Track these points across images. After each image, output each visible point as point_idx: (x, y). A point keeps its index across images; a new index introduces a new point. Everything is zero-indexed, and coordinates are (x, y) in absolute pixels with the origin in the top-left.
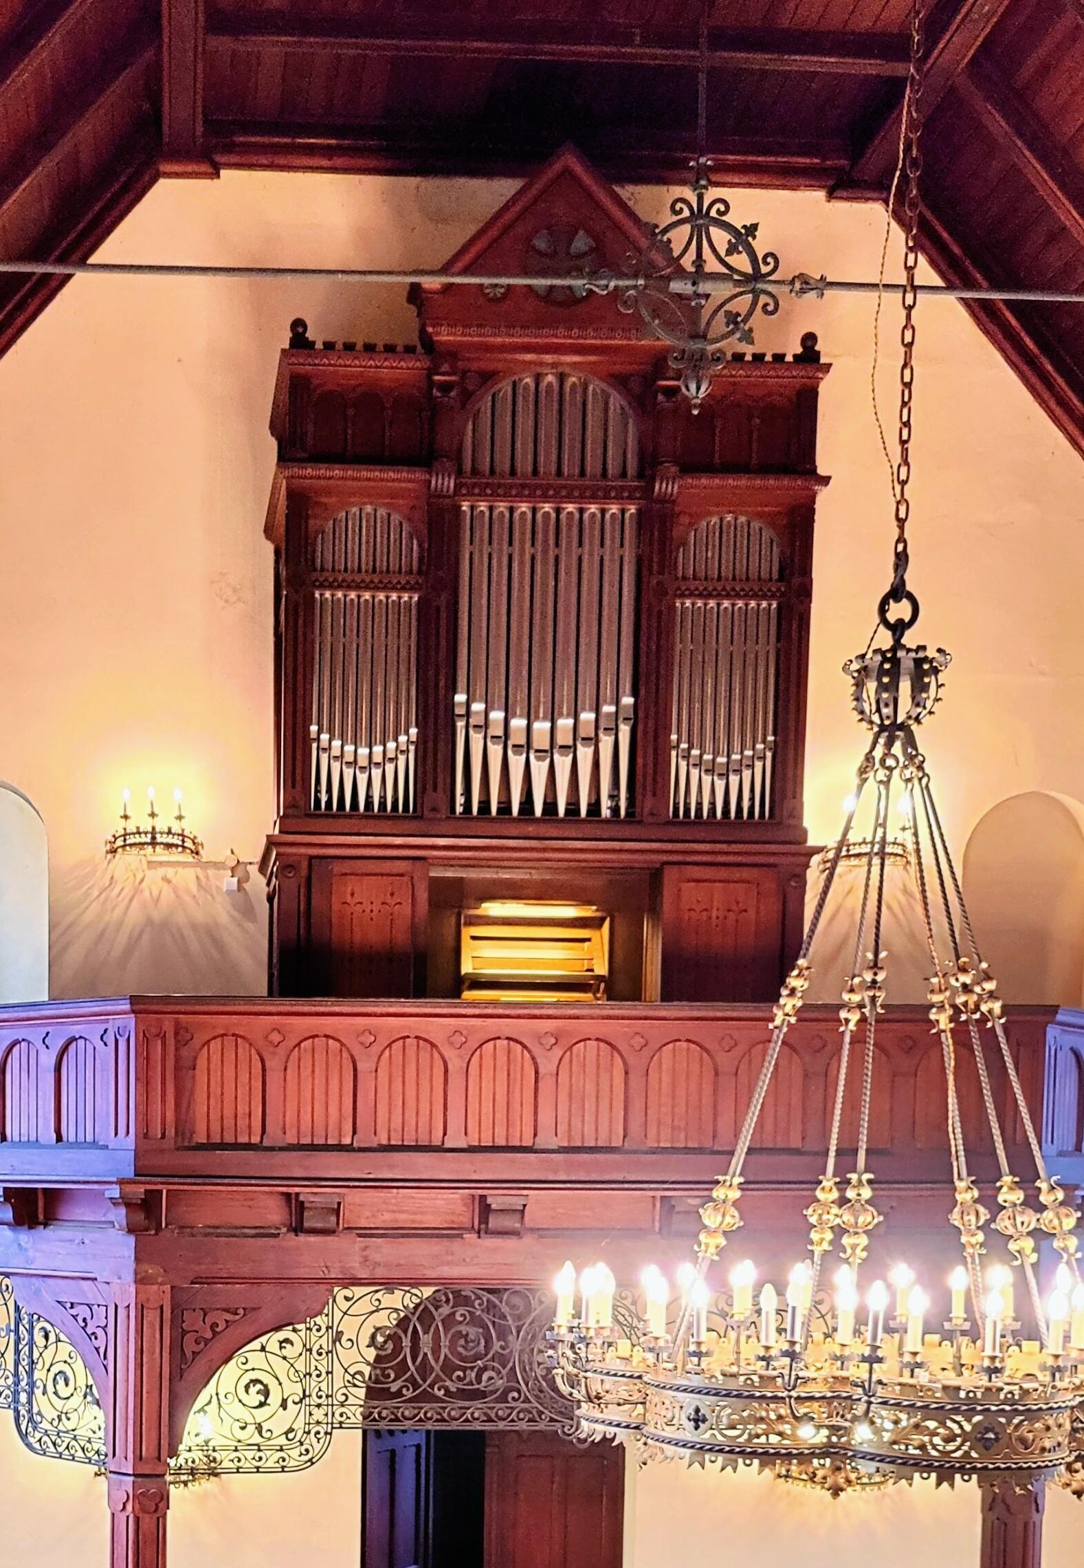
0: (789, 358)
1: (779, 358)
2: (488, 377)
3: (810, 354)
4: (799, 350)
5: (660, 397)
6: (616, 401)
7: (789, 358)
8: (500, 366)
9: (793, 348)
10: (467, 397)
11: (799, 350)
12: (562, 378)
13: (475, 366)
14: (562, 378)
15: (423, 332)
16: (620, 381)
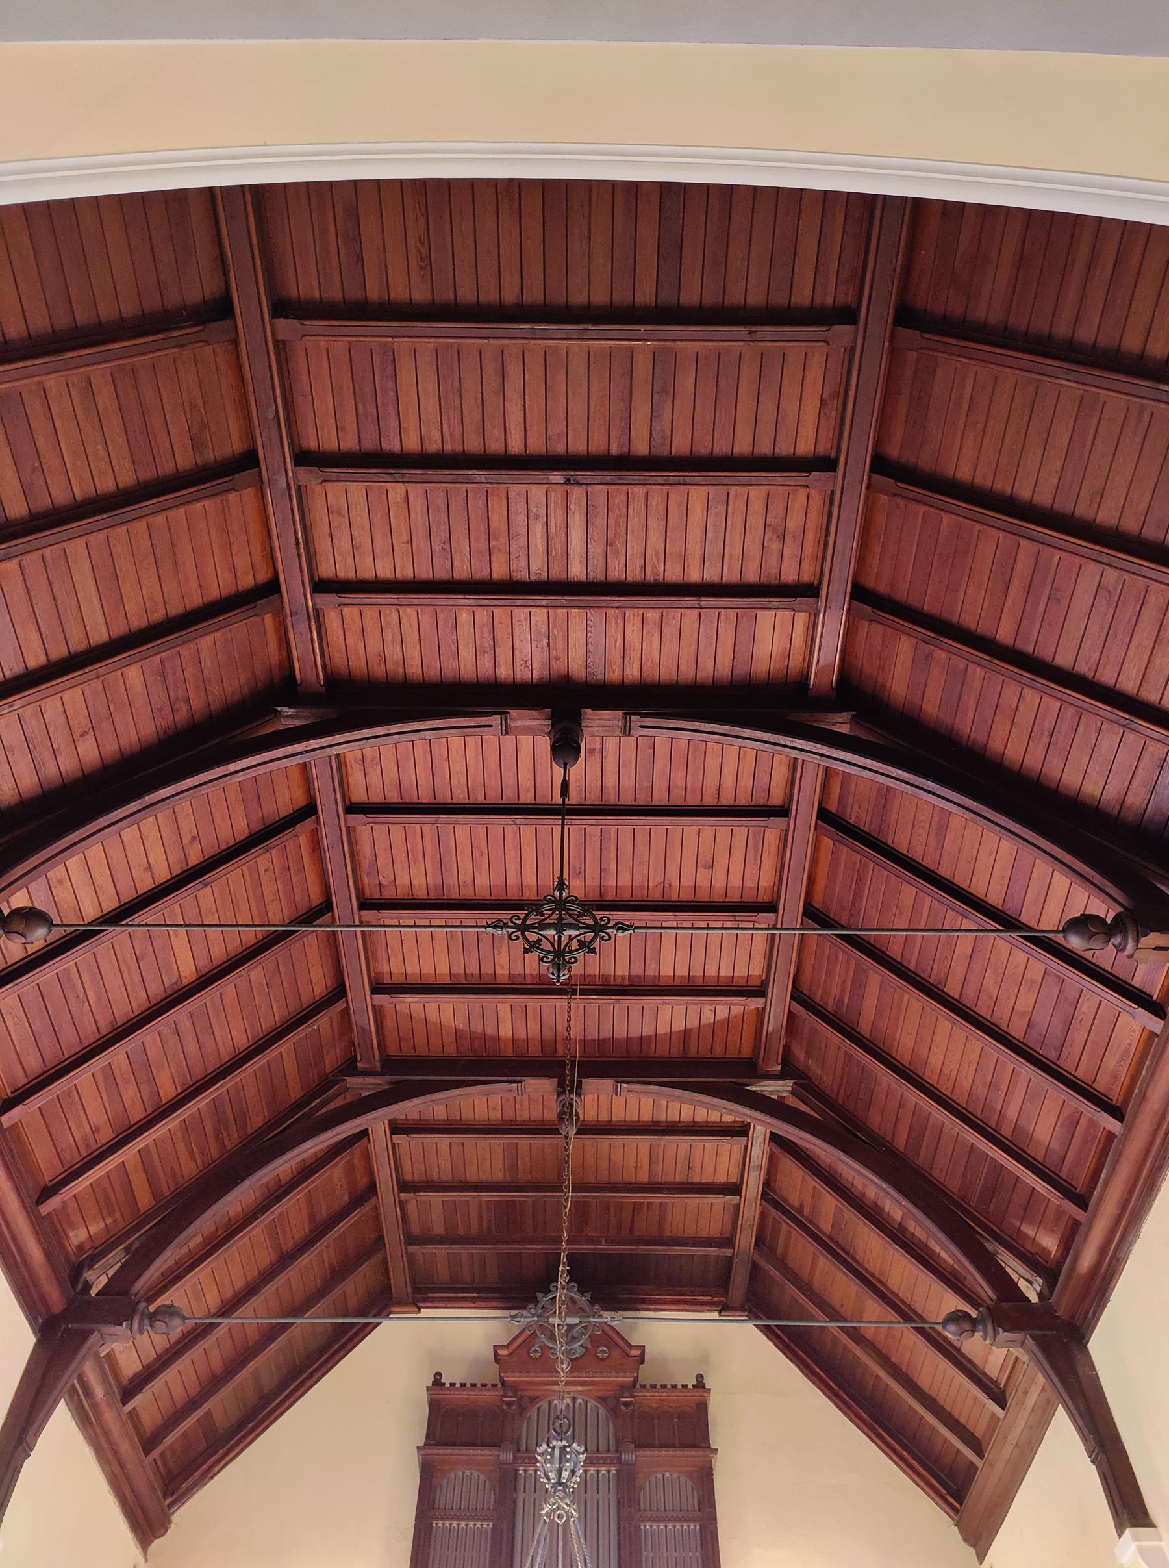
0: (690, 1387)
1: (685, 1386)
2: (533, 1400)
3: (700, 1384)
4: (695, 1382)
5: (623, 1407)
6: (602, 1411)
7: (690, 1387)
8: (536, 1394)
9: (692, 1382)
10: (522, 1410)
11: (695, 1382)
12: (574, 1399)
13: (528, 1393)
14: (574, 1399)
15: (503, 1382)
16: (603, 1400)
